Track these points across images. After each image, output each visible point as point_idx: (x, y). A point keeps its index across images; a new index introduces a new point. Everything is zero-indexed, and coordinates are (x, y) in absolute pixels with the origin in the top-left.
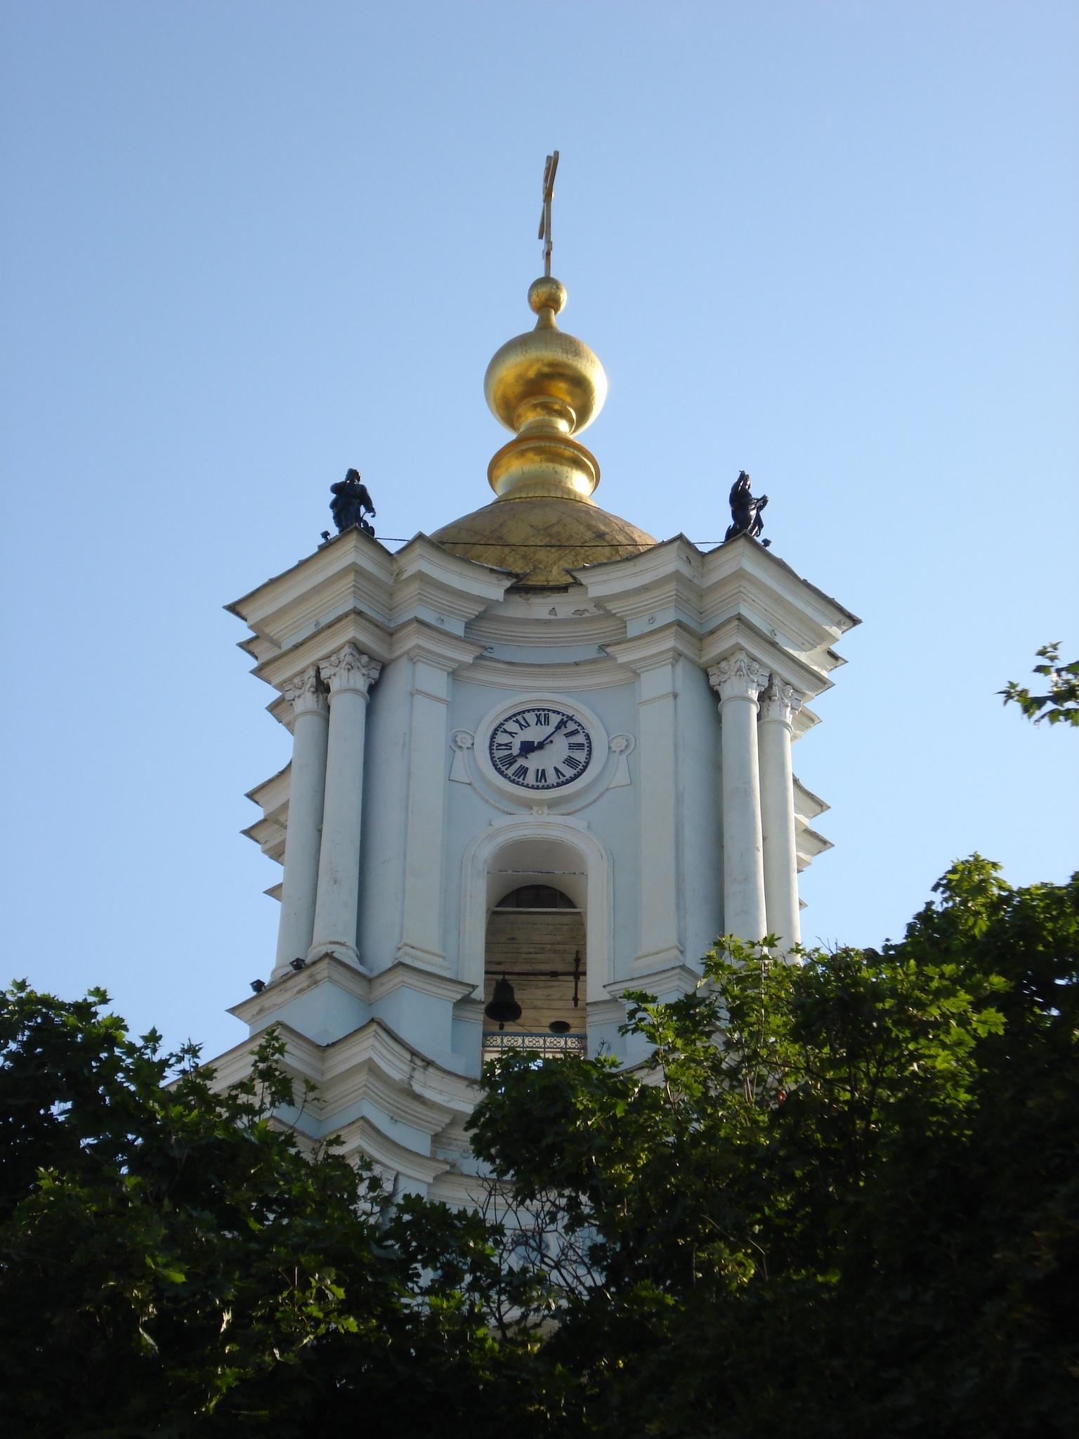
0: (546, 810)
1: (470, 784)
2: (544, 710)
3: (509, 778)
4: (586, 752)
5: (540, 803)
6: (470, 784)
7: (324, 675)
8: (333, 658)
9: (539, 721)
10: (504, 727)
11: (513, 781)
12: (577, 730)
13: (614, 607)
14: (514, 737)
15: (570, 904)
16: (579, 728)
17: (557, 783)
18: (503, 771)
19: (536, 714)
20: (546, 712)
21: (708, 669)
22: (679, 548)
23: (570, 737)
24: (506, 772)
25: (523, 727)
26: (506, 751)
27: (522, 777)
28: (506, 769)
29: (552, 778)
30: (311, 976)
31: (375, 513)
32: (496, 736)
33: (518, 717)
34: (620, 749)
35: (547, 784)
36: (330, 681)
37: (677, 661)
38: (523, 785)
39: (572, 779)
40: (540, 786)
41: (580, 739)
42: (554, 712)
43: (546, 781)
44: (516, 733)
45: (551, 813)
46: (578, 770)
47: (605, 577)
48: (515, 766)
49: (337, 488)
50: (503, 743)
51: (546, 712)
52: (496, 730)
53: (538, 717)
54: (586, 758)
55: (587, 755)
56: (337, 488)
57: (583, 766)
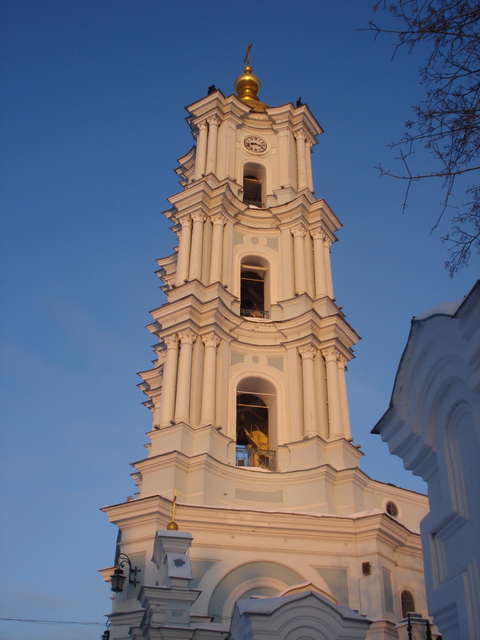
0: (256, 157)
5: (256, 155)
7: (208, 121)
8: (211, 118)
13: (273, 118)
22: (290, 105)
29: (258, 150)
30: (207, 178)
33: (251, 138)
37: (287, 129)
39: (263, 152)
41: (264, 144)
42: (258, 138)
47: (272, 111)
48: (250, 147)
49: (209, 88)
52: (245, 140)
53: (255, 139)
56: (209, 88)
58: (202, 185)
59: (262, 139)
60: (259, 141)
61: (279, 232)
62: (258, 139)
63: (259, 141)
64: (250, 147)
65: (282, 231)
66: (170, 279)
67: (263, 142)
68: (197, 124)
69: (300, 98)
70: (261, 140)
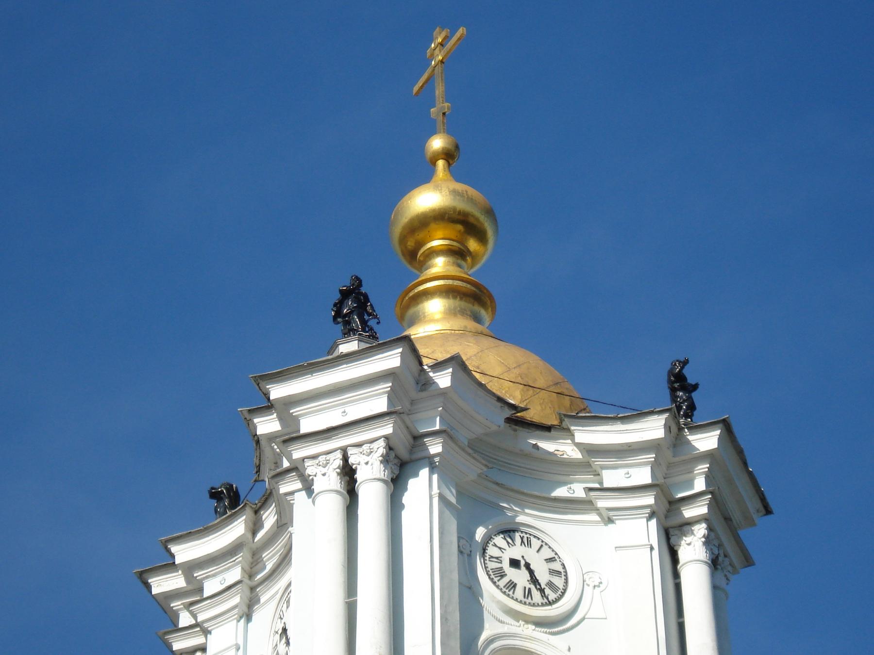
1: (470, 588)
2: (526, 533)
3: (501, 589)
4: (563, 580)
6: (470, 588)
9: (522, 541)
10: (494, 541)
11: (504, 593)
12: (554, 558)
14: (503, 552)
16: (556, 557)
17: (542, 603)
19: (520, 536)
20: (528, 536)
23: (548, 563)
24: (498, 583)
25: (510, 545)
26: (497, 564)
27: (512, 590)
31: (378, 319)
32: (488, 548)
36: (359, 467)
38: (512, 598)
39: (557, 600)
40: (527, 603)
41: (557, 566)
42: (535, 537)
45: (537, 629)
48: (505, 580)
51: (528, 536)
53: (522, 538)
54: (564, 586)
55: (564, 582)
57: (562, 592)
59: (547, 539)
60: (538, 551)
62: (536, 543)
63: (538, 551)
64: (505, 580)
67: (552, 555)
68: (303, 459)
70: (545, 548)
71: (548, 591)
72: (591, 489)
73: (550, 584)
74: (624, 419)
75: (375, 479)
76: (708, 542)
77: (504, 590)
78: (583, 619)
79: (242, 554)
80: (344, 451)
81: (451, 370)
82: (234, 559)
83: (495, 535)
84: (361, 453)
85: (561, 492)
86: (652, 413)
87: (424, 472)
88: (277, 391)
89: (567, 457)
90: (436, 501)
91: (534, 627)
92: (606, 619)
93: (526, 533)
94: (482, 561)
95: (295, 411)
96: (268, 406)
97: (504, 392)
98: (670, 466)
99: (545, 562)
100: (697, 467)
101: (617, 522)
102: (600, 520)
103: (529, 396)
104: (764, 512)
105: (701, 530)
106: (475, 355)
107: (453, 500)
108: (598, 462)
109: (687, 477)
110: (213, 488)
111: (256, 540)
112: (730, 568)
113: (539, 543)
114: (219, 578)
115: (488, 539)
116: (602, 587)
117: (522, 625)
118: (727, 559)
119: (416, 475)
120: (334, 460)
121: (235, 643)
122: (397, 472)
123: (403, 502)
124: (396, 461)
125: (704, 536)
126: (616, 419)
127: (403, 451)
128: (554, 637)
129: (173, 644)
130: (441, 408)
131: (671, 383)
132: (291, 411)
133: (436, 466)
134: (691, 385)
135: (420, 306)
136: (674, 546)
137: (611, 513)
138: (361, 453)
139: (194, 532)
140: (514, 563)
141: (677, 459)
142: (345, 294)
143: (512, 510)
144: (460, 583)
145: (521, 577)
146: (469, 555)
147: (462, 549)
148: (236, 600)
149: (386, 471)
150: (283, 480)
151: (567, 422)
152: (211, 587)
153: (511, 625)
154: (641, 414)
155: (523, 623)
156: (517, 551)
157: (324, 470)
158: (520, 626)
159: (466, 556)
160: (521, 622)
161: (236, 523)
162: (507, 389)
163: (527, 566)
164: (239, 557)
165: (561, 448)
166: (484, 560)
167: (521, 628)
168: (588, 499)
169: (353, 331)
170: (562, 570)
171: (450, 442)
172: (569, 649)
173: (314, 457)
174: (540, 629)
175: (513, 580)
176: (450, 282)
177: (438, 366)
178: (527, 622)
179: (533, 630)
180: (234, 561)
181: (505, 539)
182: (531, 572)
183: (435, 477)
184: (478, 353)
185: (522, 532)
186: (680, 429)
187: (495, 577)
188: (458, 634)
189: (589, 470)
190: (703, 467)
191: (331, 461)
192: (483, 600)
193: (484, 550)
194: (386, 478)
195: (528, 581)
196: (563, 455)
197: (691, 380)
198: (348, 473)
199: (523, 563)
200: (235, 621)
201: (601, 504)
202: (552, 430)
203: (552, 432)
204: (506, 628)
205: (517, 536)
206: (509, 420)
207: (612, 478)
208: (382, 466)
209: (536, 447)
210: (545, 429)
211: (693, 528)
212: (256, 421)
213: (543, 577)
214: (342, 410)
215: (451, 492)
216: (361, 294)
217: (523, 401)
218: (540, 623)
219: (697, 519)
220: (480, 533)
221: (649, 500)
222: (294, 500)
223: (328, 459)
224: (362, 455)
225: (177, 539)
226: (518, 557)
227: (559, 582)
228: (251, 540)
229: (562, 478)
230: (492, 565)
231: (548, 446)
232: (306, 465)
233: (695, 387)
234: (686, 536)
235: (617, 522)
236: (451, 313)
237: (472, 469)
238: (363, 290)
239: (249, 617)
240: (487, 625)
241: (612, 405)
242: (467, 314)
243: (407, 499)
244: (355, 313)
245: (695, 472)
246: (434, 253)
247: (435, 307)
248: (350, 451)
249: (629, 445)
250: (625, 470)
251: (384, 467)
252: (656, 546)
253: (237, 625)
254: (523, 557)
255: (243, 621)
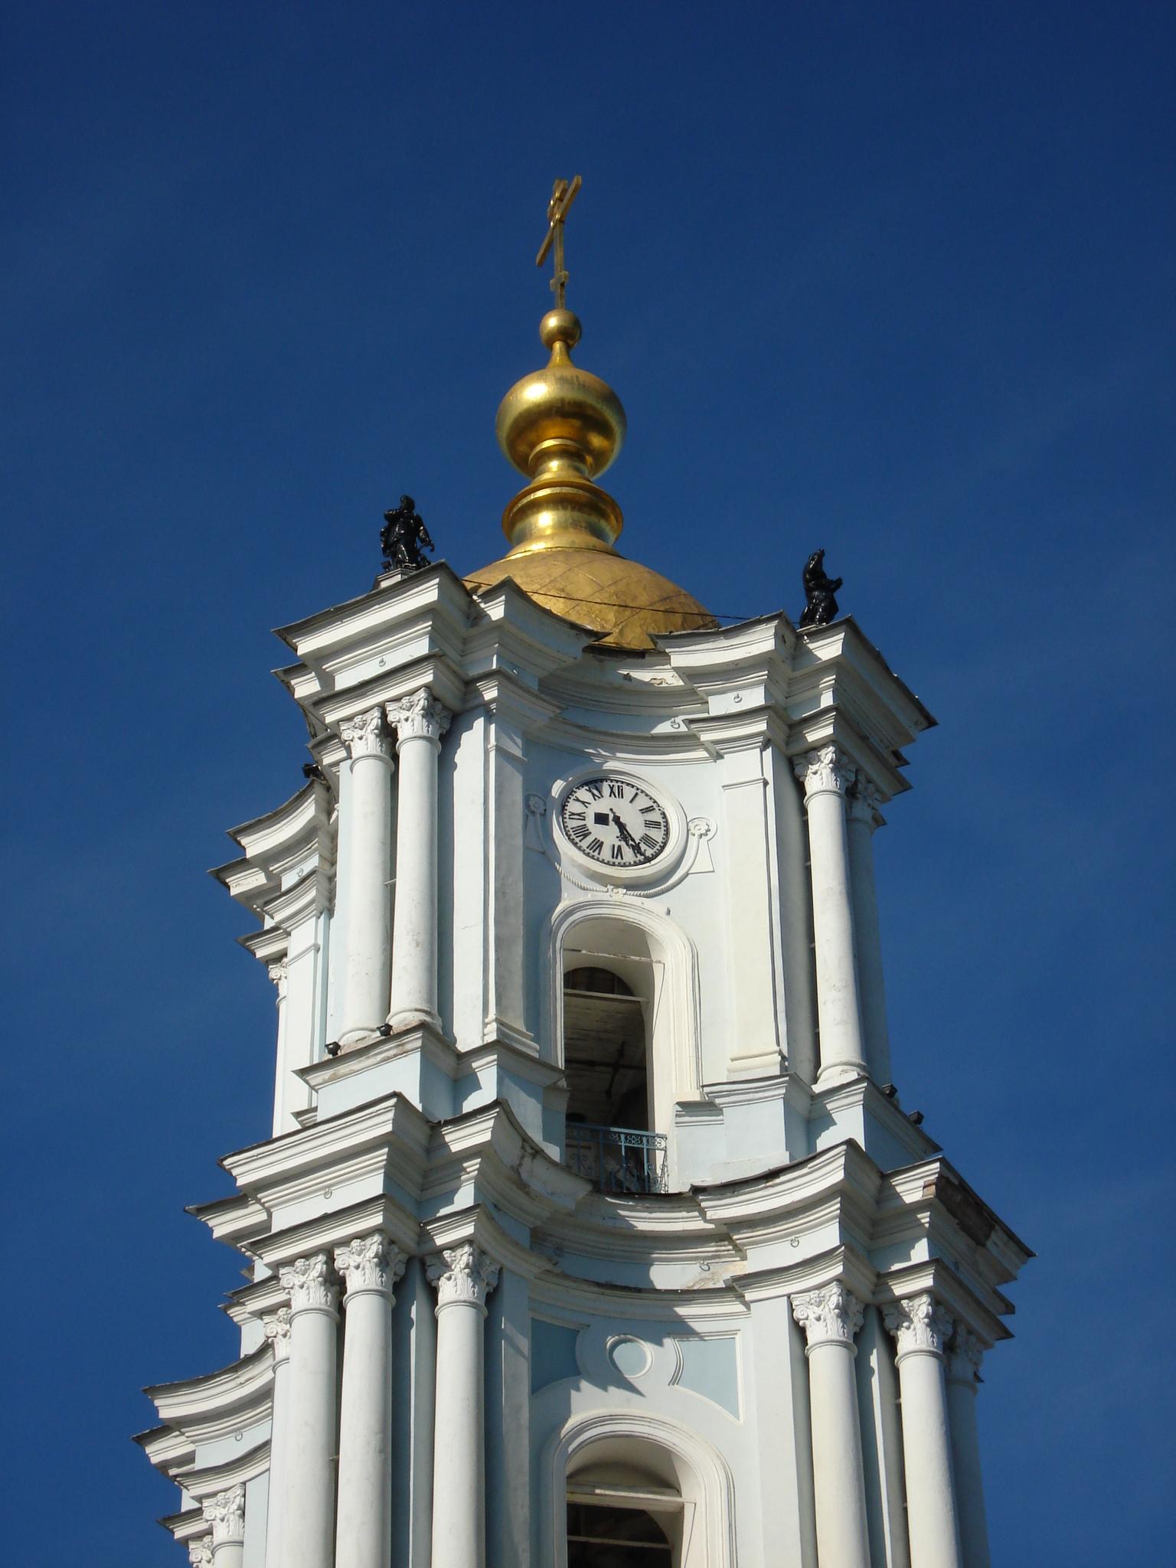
1: (543, 853)
2: (617, 781)
4: (663, 832)
6: (543, 853)
7: (390, 718)
8: (405, 701)
9: (612, 792)
10: (576, 795)
11: (588, 855)
12: (652, 806)
14: (587, 807)
15: (626, 989)
16: (655, 805)
17: (635, 862)
18: (577, 843)
19: (610, 785)
20: (620, 784)
21: (795, 758)
23: (646, 814)
24: (580, 844)
25: (596, 798)
27: (598, 850)
28: (580, 841)
31: (432, 545)
32: (569, 804)
34: (699, 832)
35: (624, 861)
36: (399, 725)
38: (598, 860)
40: (617, 864)
41: (655, 816)
42: (628, 784)
43: (622, 858)
44: (589, 803)
45: (629, 892)
46: (655, 849)
48: (590, 839)
50: (576, 812)
51: (620, 784)
53: (612, 788)
54: (663, 839)
57: (660, 846)
58: (387, 1110)
60: (631, 802)
61: (741, 1308)
62: (629, 792)
64: (590, 839)
65: (752, 1305)
66: (214, 1495)
67: (651, 803)
68: (338, 722)
69: (822, 554)
70: (641, 796)
71: (643, 847)
72: (692, 721)
73: (646, 839)
74: (728, 633)
75: (415, 737)
76: (837, 767)
77: (588, 851)
78: (687, 874)
79: (317, 839)
80: (382, 708)
81: (503, 597)
82: (310, 846)
83: (578, 788)
84: (401, 708)
85: (664, 728)
86: (759, 622)
87: (479, 724)
88: (306, 646)
89: (666, 685)
90: (492, 755)
91: (625, 890)
92: (713, 871)
93: (617, 781)
94: (561, 819)
95: (328, 666)
96: (301, 667)
97: (593, 616)
98: (791, 682)
99: (640, 813)
100: (822, 680)
101: (725, 756)
102: (708, 756)
103: (626, 618)
104: (925, 723)
105: (828, 754)
106: (561, 576)
107: (518, 753)
108: (702, 688)
109: (808, 694)
110: (307, 765)
111: (331, 822)
112: (877, 796)
113: (634, 791)
114: (297, 870)
115: (568, 794)
116: (710, 835)
117: (610, 890)
118: (871, 786)
119: (471, 728)
120: (372, 720)
121: (312, 942)
122: (447, 726)
123: (456, 760)
124: (445, 713)
125: (831, 762)
126: (718, 634)
127: (451, 699)
128: (650, 899)
129: (256, 951)
130: (497, 645)
131: (806, 581)
132: (324, 667)
133: (494, 714)
134: (832, 582)
135: (527, 521)
136: (800, 776)
137: (718, 747)
138: (401, 708)
139: (264, 819)
140: (601, 819)
141: (797, 674)
142: (392, 519)
143: (599, 755)
144: (527, 848)
145: (609, 835)
146: (544, 814)
147: (533, 809)
148: (312, 894)
149: (430, 726)
150: (325, 749)
151: (661, 644)
152: (288, 881)
153: (596, 891)
154: (744, 625)
155: (612, 887)
156: (603, 805)
157: (362, 733)
158: (607, 892)
159: (538, 815)
160: (610, 887)
161: (306, 804)
162: (597, 612)
163: (617, 820)
164: (315, 844)
165: (659, 675)
166: (564, 818)
167: (608, 894)
168: (691, 733)
169: (400, 562)
170: (661, 821)
171: (511, 687)
172: (669, 912)
173: (349, 719)
174: (632, 893)
175: (598, 838)
176: (557, 490)
177: (490, 595)
178: (617, 886)
179: (625, 894)
180: (309, 849)
181: (590, 791)
182: (622, 827)
183: (493, 727)
184: (565, 572)
185: (612, 781)
186: (799, 637)
187: (577, 837)
188: (521, 910)
189: (696, 698)
190: (829, 680)
191: (369, 721)
192: (560, 865)
193: (564, 807)
194: (429, 735)
195: (617, 837)
196: (661, 683)
197: (831, 574)
198: (388, 733)
199: (611, 816)
200: (314, 918)
201: (705, 737)
202: (647, 656)
203: (646, 658)
204: (589, 895)
205: (606, 788)
206: (590, 649)
207: (720, 704)
208: (424, 720)
209: (628, 677)
210: (639, 656)
211: (819, 754)
212: (293, 682)
213: (637, 831)
214: (380, 659)
215: (516, 744)
216: (412, 518)
217: (618, 625)
218: (632, 886)
219: (822, 742)
220: (557, 787)
221: (761, 726)
222: (338, 771)
223: (364, 719)
224: (402, 711)
225: (248, 830)
226: (606, 811)
227: (657, 835)
228: (326, 822)
229: (663, 712)
230: (572, 824)
231: (643, 675)
232: (342, 728)
233: (838, 583)
234: (812, 764)
235: (725, 756)
236: (561, 527)
237: (541, 714)
238: (416, 512)
239: (330, 912)
240: (565, 895)
241: (725, 617)
242: (581, 527)
243: (460, 757)
244: (402, 540)
245: (821, 686)
246: (548, 454)
247: (545, 520)
248: (389, 707)
249: (735, 663)
250: (735, 694)
251: (427, 721)
252: (770, 780)
253: (317, 922)
254: (611, 810)
255: (322, 917)
